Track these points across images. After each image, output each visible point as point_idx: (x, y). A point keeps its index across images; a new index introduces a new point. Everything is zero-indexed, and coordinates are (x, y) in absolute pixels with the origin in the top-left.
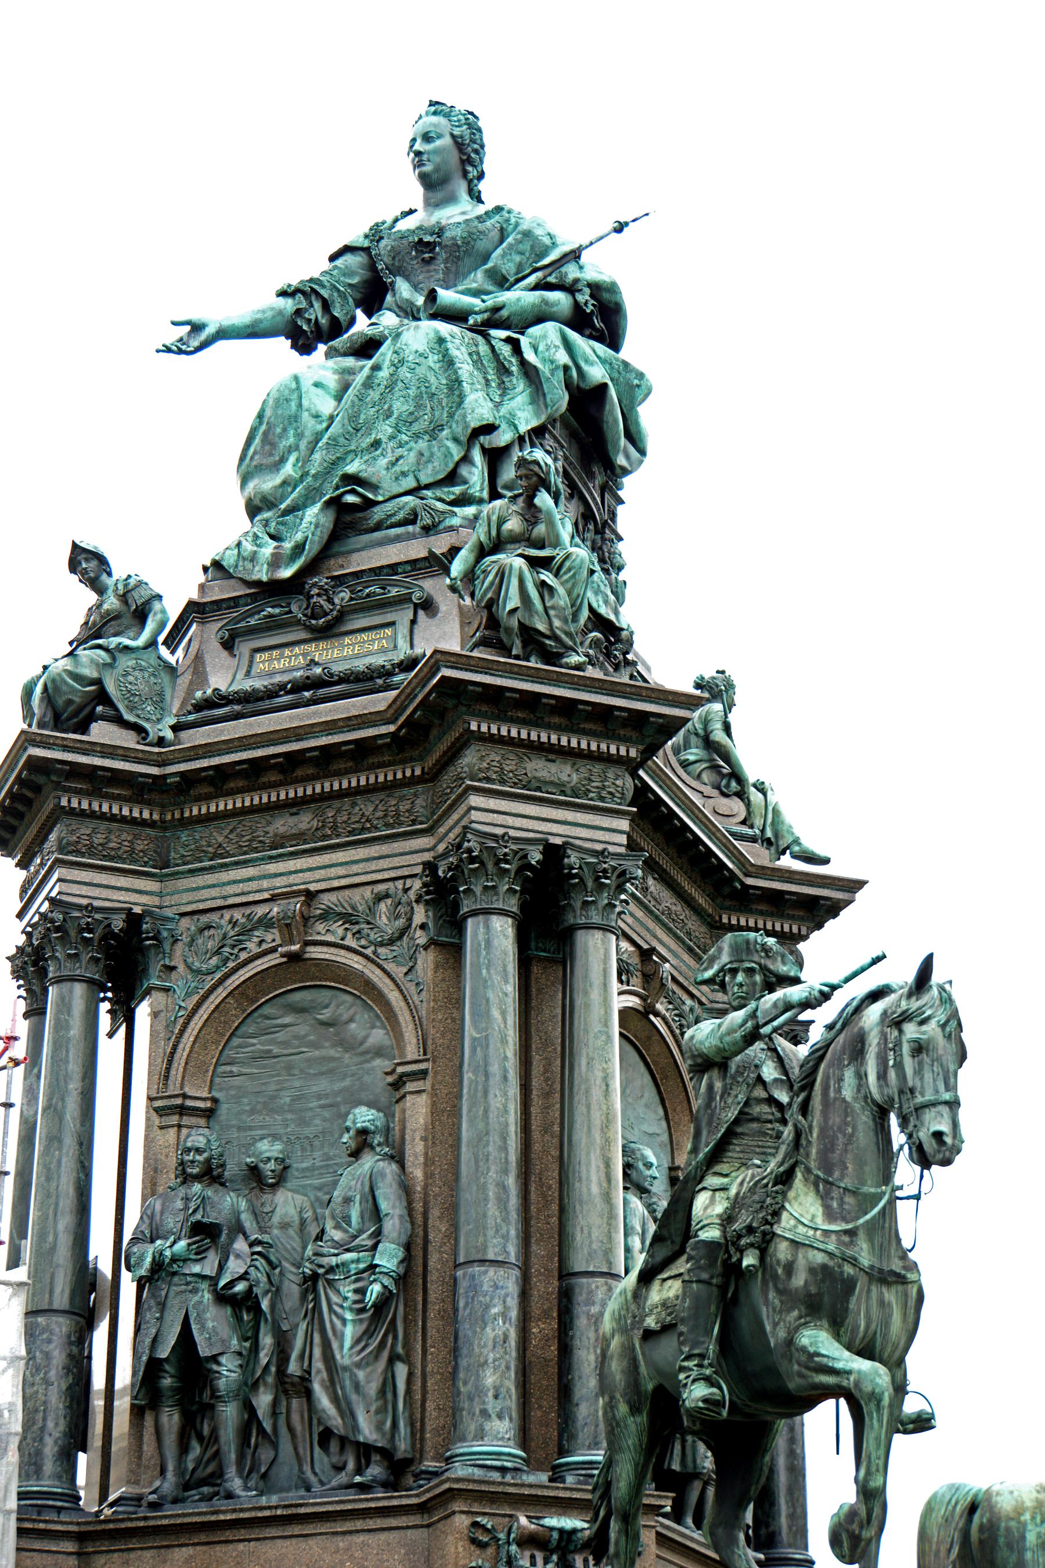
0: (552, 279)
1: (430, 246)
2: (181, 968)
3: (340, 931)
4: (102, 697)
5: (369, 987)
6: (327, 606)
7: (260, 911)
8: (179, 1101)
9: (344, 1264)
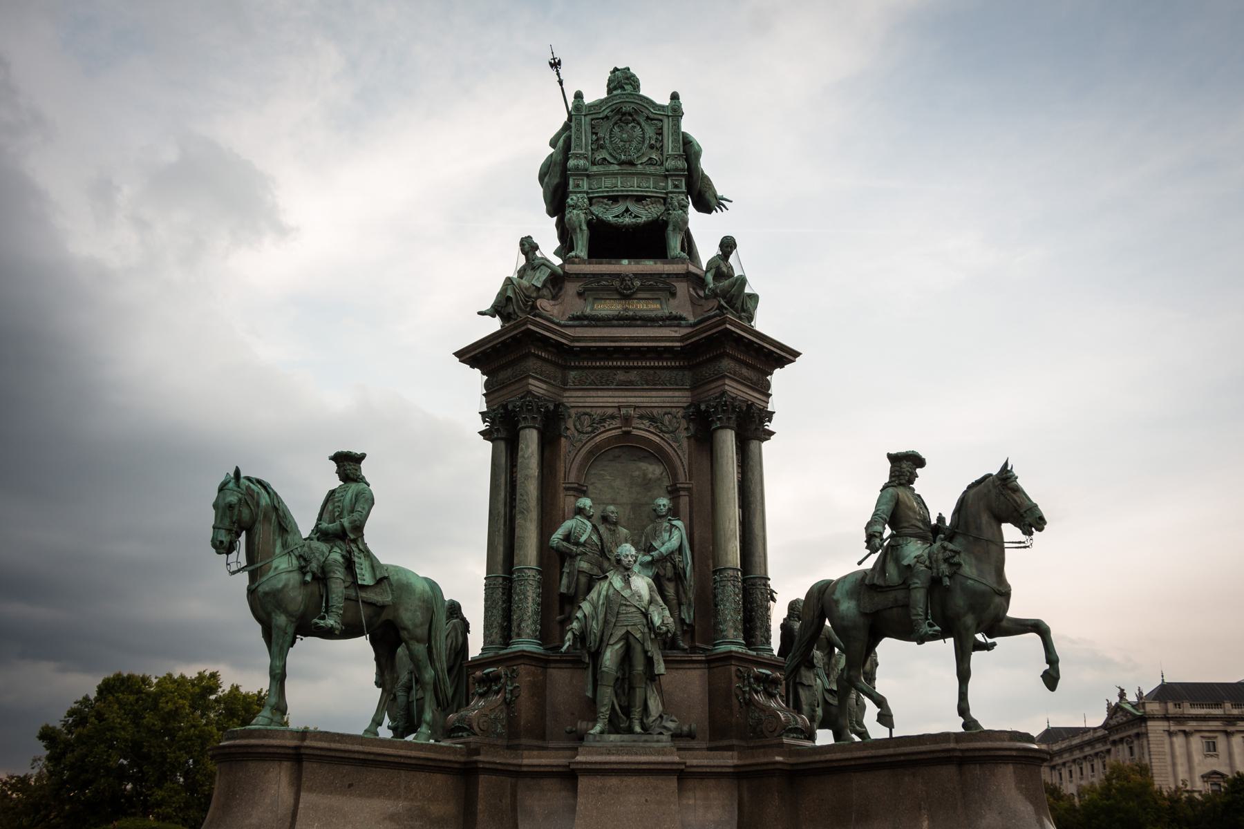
3: (648, 424)
6: (631, 286)
7: (610, 411)
8: (576, 485)
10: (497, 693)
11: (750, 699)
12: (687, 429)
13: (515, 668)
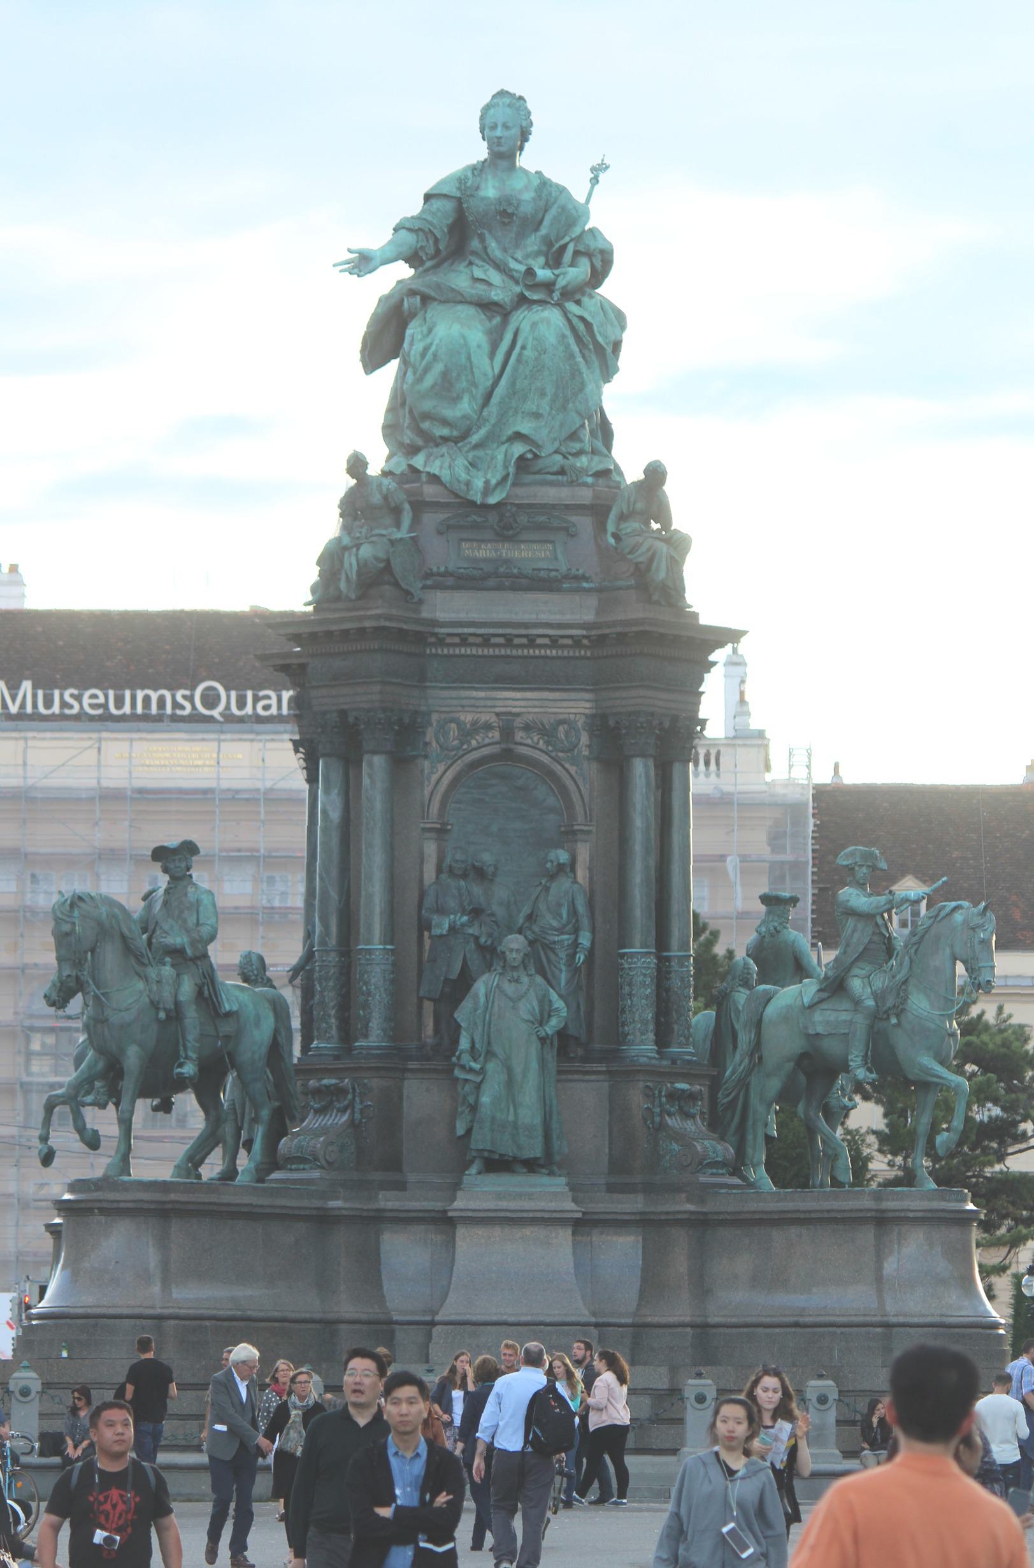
0: (581, 248)
1: (511, 215)
2: (434, 744)
3: (535, 739)
4: (388, 568)
5: (551, 774)
6: (515, 525)
7: (484, 718)
8: (438, 826)
9: (562, 941)
10: (343, 1111)
11: (661, 1123)
12: (589, 746)
13: (366, 1081)
